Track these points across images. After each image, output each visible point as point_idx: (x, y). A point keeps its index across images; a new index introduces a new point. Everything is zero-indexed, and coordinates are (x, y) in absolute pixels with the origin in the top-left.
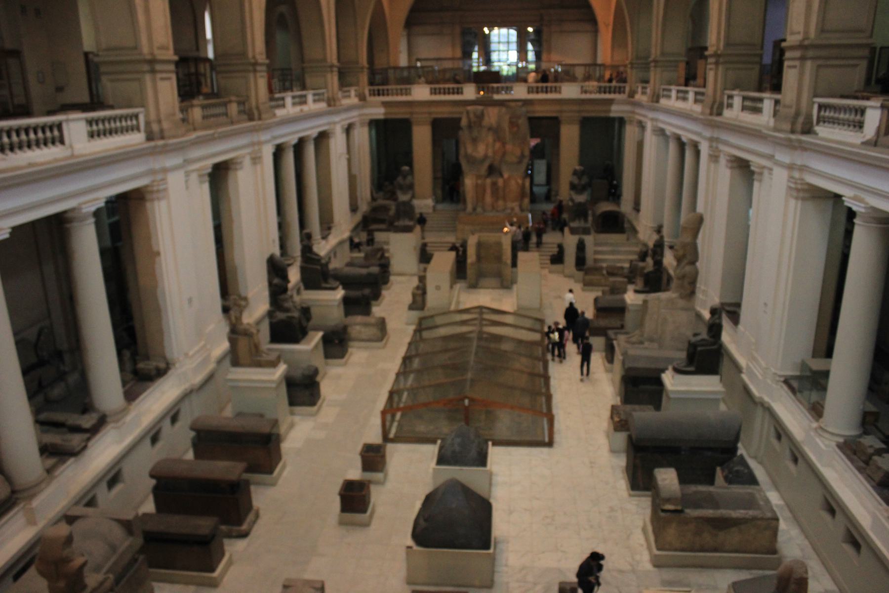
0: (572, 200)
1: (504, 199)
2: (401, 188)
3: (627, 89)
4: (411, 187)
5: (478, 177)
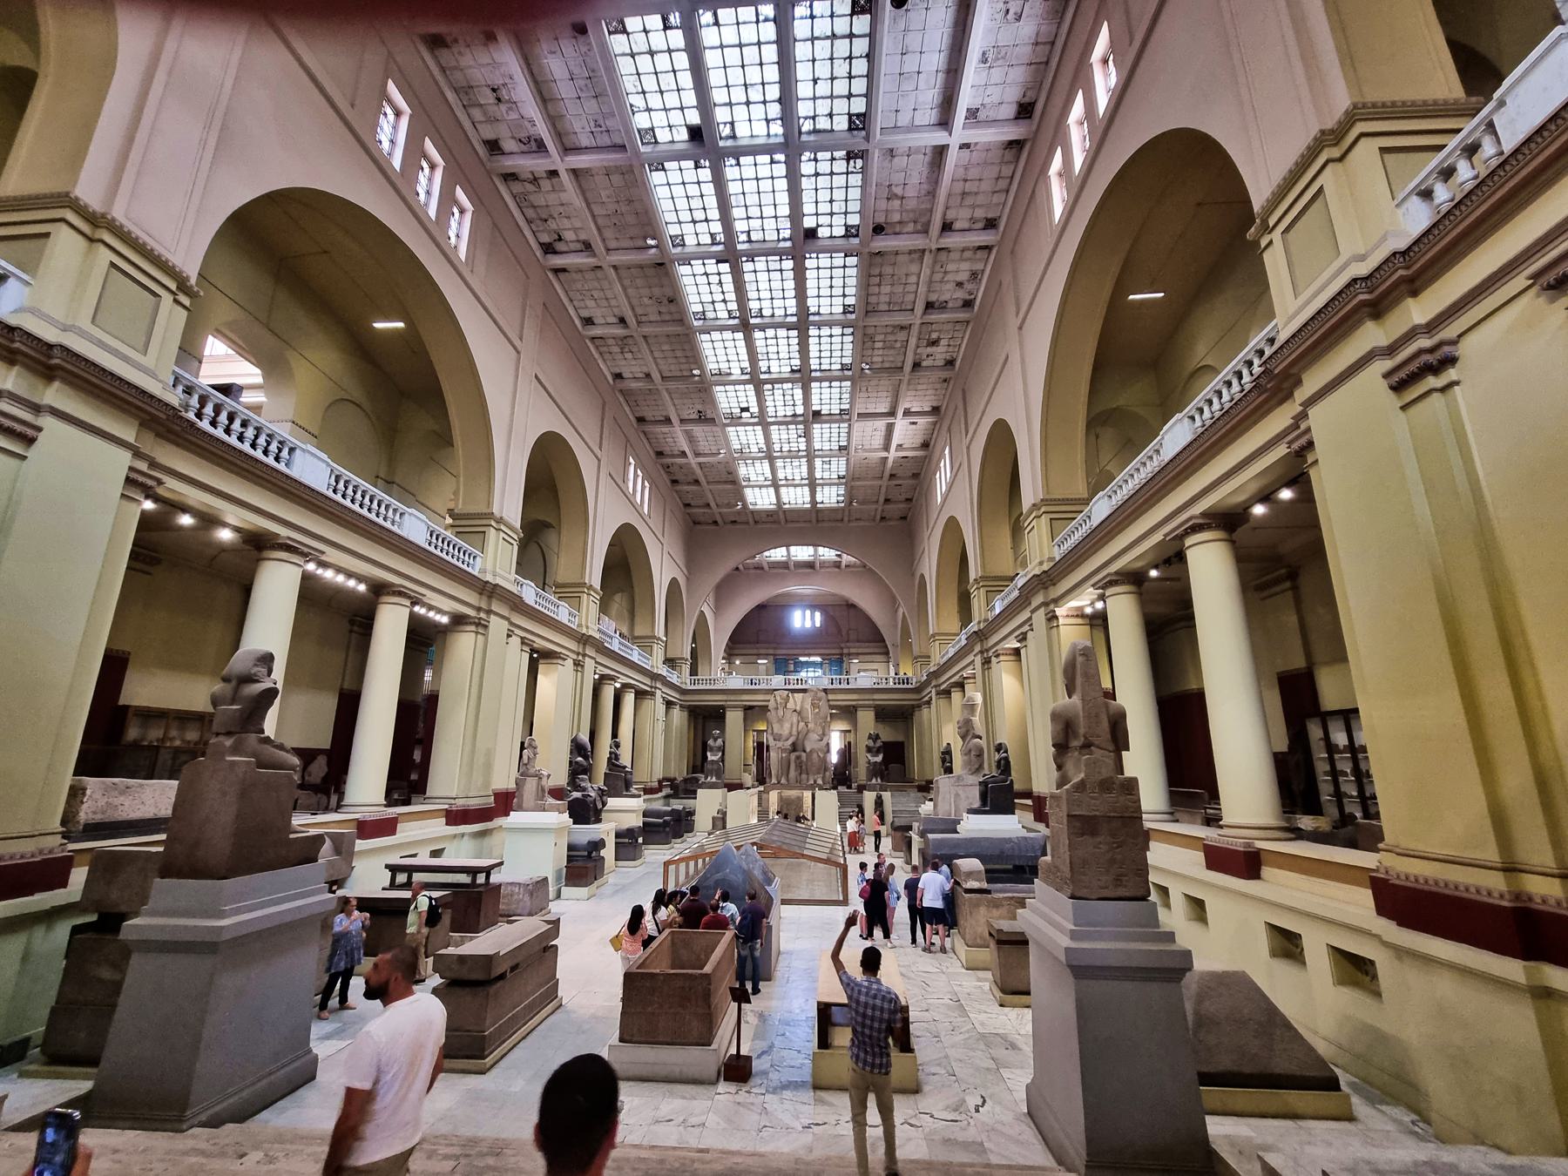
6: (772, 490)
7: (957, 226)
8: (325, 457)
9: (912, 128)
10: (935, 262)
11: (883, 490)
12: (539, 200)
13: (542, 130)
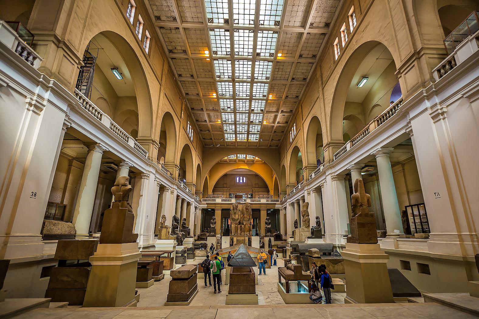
0: (266, 227)
1: (244, 232)
2: (212, 223)
3: (280, 201)
4: (215, 223)
5: (236, 224)
6: (234, 136)
7: (303, 56)
8: (110, 118)
9: (294, 27)
10: (296, 66)
11: (272, 136)
12: (171, 36)
13: (176, 14)
